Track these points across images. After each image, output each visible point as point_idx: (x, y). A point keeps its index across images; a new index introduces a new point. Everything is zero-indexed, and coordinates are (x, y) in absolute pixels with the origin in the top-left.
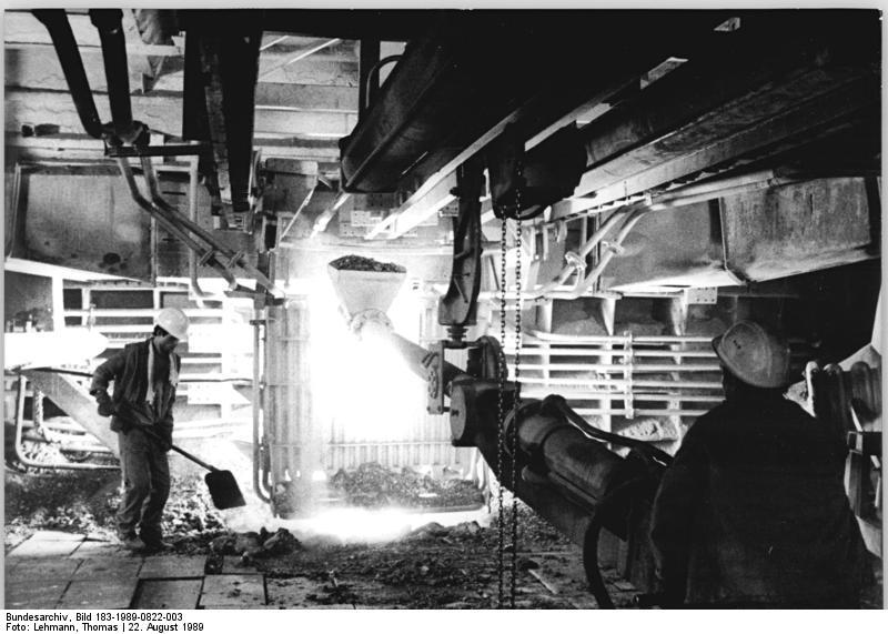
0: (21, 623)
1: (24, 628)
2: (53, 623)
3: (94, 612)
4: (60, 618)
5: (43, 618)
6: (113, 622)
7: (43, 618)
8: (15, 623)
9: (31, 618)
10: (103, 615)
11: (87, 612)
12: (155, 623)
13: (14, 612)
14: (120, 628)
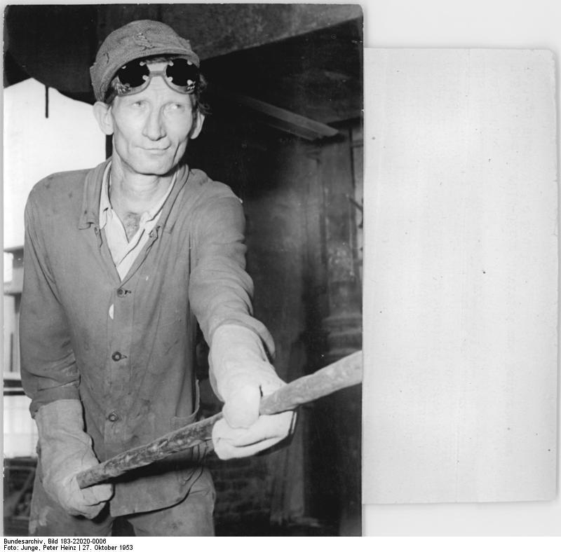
0: (13, 545)
1: (15, 548)
2: (33, 545)
3: (59, 538)
4: (38, 542)
5: (27, 542)
6: (71, 544)
7: (27, 542)
8: (10, 545)
9: (20, 542)
10: (65, 540)
11: (55, 538)
12: (101, 545)
13: (9, 538)
14: (77, 548)
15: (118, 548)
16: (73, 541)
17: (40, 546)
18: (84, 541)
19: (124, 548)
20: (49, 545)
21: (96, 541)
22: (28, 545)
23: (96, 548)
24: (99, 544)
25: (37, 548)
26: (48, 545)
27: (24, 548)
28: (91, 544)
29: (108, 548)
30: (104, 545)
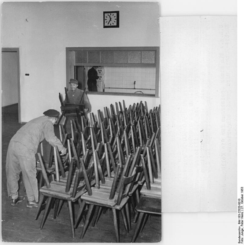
0: (241, 239)
2: (241, 230)
4: (240, 229)
5: (240, 233)
6: (241, 214)
7: (240, 233)
8: (241, 241)
9: (239, 236)
10: (239, 216)
14: (242, 211)
15: (242, 193)
16: (239, 213)
17: (241, 227)
18: (239, 208)
19: (242, 191)
20: (241, 223)
21: (239, 203)
22: (241, 233)
23: (242, 203)
24: (240, 203)
25: (242, 229)
26: (241, 224)
27: (242, 235)
28: (241, 205)
29: (242, 198)
30: (241, 199)
